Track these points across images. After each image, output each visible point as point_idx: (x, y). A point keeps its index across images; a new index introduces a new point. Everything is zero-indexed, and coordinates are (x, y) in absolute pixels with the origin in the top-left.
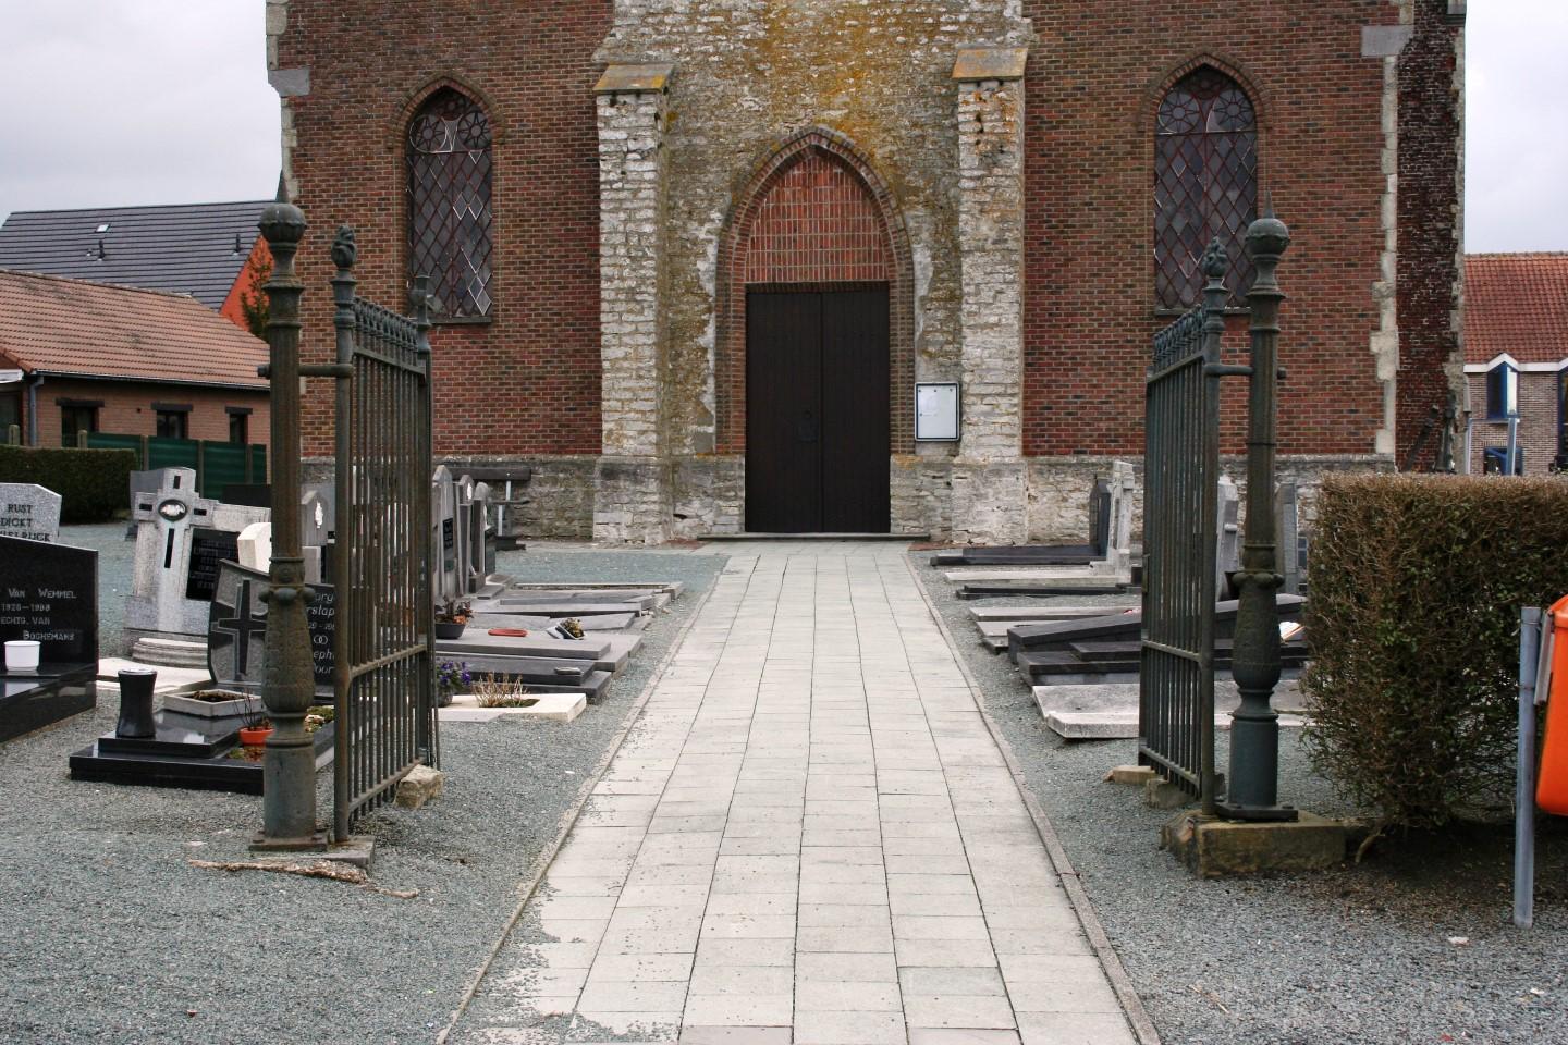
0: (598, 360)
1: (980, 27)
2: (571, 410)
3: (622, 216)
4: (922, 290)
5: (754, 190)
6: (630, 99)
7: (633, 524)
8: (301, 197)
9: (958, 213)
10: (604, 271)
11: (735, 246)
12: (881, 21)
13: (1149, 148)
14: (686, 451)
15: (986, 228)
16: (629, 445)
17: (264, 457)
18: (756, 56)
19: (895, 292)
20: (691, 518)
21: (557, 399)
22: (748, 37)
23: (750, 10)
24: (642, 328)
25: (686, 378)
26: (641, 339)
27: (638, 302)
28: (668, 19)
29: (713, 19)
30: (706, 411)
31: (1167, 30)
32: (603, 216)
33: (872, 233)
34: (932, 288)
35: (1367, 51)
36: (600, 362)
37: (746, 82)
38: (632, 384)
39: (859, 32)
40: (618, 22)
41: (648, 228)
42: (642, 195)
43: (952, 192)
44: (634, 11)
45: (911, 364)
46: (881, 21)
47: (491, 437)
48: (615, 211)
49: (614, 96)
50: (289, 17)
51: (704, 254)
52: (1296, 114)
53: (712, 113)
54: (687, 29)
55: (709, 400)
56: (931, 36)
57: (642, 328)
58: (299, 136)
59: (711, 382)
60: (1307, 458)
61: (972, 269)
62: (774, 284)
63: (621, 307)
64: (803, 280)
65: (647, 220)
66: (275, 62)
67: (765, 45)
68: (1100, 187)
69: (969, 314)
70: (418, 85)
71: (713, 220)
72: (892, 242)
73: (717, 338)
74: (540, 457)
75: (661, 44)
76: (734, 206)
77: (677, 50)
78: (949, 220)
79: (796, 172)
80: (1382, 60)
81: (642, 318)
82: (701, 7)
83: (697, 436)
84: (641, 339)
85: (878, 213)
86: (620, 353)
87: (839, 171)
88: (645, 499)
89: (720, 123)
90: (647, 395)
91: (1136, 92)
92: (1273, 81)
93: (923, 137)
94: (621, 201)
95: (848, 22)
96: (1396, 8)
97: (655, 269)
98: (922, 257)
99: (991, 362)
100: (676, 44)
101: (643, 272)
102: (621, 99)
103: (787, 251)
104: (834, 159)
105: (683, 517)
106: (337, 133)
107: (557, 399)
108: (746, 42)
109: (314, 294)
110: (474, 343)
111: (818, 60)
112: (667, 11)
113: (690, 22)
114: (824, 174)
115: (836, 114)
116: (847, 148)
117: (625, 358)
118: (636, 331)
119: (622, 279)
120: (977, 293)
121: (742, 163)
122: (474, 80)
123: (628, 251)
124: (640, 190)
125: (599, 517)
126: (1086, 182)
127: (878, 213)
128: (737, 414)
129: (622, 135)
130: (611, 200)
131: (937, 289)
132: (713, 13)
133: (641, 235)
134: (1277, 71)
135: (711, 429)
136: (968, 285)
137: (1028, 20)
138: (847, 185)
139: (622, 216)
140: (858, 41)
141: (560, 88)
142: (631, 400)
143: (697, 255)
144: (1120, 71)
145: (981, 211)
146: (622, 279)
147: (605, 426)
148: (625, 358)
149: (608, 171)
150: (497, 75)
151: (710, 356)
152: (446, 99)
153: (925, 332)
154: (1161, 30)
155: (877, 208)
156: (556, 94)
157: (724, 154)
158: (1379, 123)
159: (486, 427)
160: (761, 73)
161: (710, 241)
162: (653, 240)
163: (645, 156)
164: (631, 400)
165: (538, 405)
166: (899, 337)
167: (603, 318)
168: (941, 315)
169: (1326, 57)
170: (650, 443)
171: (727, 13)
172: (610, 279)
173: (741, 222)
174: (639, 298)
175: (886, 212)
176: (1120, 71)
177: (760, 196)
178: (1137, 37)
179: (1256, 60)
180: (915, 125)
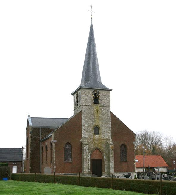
4: (105, 160)
13: (120, 149)
15: (112, 155)
17: (39, 173)
35: (133, 143)
61: (111, 158)
70: (66, 142)
122: (70, 142)
138: (99, 152)
149: (84, 150)
152: (68, 143)
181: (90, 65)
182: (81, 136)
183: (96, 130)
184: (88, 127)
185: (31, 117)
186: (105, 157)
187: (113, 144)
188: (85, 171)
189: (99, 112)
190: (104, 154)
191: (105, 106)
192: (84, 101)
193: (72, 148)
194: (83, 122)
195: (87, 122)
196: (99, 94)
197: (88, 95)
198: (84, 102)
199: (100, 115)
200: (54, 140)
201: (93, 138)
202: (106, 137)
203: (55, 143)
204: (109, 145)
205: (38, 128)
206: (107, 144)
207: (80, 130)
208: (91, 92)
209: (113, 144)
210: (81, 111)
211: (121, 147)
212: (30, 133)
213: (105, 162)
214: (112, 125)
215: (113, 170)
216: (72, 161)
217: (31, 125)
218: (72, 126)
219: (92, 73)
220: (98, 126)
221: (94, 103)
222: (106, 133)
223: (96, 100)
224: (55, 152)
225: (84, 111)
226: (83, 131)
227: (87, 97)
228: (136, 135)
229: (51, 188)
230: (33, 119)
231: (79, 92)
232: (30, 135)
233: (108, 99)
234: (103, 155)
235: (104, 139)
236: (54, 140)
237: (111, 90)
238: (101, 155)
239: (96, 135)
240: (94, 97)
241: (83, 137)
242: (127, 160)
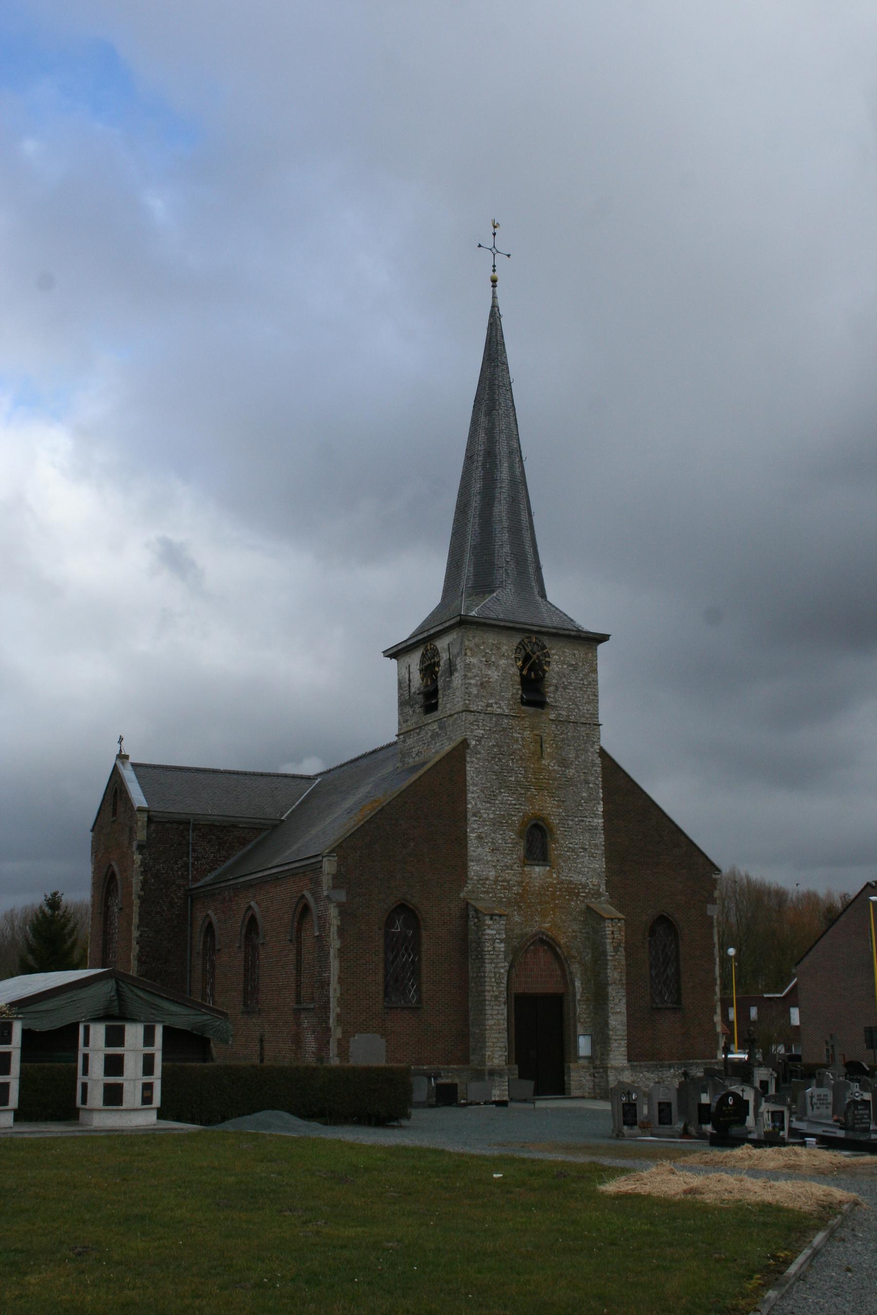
1: (593, 895)
4: (578, 997)
6: (497, 918)
13: (647, 945)
15: (616, 975)
16: (496, 1061)
24: (500, 1012)
26: (500, 1017)
28: (487, 882)
32: (487, 965)
34: (582, 996)
37: (515, 910)
38: (497, 1035)
39: (554, 893)
41: (502, 971)
48: (491, 963)
49: (492, 916)
57: (500, 1012)
58: (342, 920)
60: (699, 1061)
61: (611, 990)
63: (493, 1003)
67: (521, 895)
74: (441, 1066)
84: (500, 1017)
90: (502, 1040)
93: (576, 936)
94: (493, 959)
99: (619, 1027)
100: (490, 893)
102: (494, 917)
111: (540, 903)
112: (487, 879)
115: (547, 925)
116: (553, 940)
118: (498, 1014)
119: (493, 991)
129: (494, 932)
132: (503, 881)
133: (500, 973)
146: (493, 991)
149: (488, 947)
160: (520, 907)
163: (502, 941)
168: (584, 1007)
172: (489, 991)
180: (573, 931)
181: (496, 510)
182: (465, 868)
183: (537, 840)
184: (497, 824)
185: (135, 766)
186: (578, 984)
187: (621, 916)
188: (491, 1058)
190: (575, 968)
191: (572, 718)
192: (475, 691)
193: (424, 934)
194: (474, 798)
195: (490, 798)
196: (547, 655)
198: (476, 696)
199: (553, 765)
200: (334, 887)
201: (520, 883)
202: (584, 880)
203: (340, 905)
204: (603, 919)
205: (180, 823)
206: (592, 916)
207: (462, 841)
208: (508, 645)
209: (621, 916)
210: (466, 740)
211: (652, 932)
212: (141, 848)
213: (581, 1010)
214: (606, 815)
215: (624, 1049)
216: (419, 1001)
217: (145, 805)
218: (409, 812)
219: (507, 549)
220: (543, 819)
221: (524, 702)
222: (583, 860)
223: (533, 689)
224: (340, 951)
225: (479, 740)
226: (474, 849)
227: (485, 671)
228: (719, 870)
229: (788, 1177)
230: (138, 769)
231: (441, 644)
232: (137, 858)
233: (590, 683)
234: (571, 973)
235: (572, 891)
236: (334, 887)
237: (604, 638)
238: (559, 973)
239: (537, 869)
240: (525, 672)
241: (471, 874)
242: (678, 1001)
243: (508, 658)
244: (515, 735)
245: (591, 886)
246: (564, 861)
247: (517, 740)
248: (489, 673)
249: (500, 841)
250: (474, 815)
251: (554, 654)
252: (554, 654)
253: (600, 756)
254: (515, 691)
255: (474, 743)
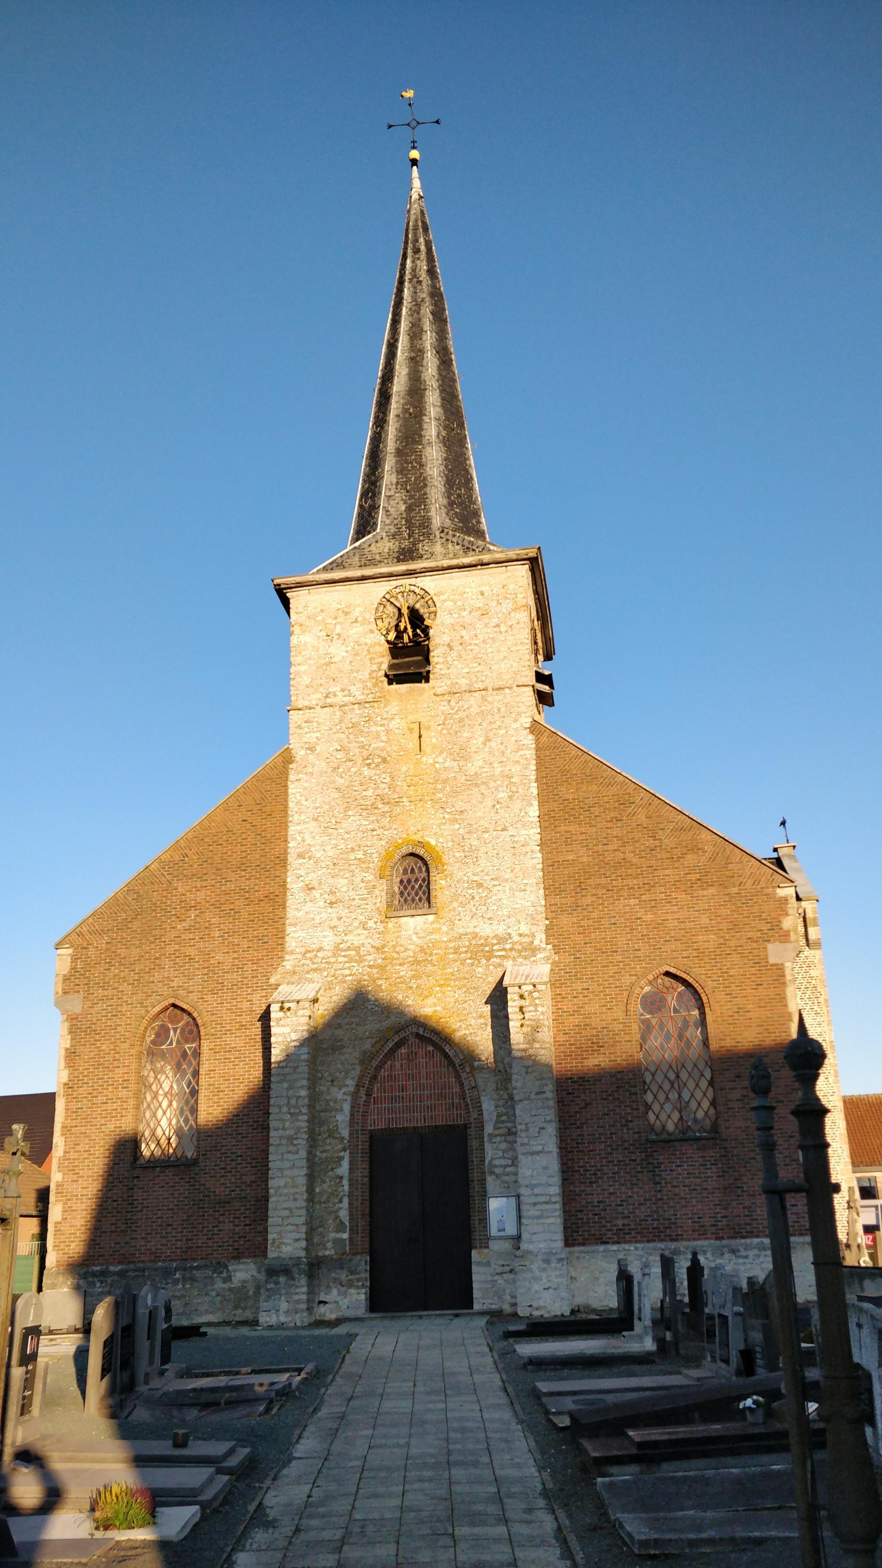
0: (267, 1189)
1: (519, 951)
2: (247, 1225)
3: (285, 1085)
4: (489, 1129)
5: (375, 1063)
7: (288, 1311)
8: (70, 1081)
9: (511, 1075)
10: (272, 1124)
11: (362, 1103)
12: (456, 951)
14: (327, 1253)
18: (376, 975)
19: (472, 1131)
20: (330, 1303)
21: (238, 1218)
22: (371, 963)
23: (373, 947)
25: (328, 1201)
26: (296, 1172)
27: (295, 1145)
28: (320, 954)
29: (347, 953)
30: (342, 1223)
31: (639, 950)
33: (454, 1090)
35: (772, 960)
36: (268, 1189)
40: (287, 957)
42: (298, 1070)
43: (507, 1060)
44: (298, 950)
45: (483, 1182)
46: (456, 951)
47: (190, 1247)
50: (72, 962)
51: (342, 1109)
52: (730, 1001)
53: (348, 1013)
54: (332, 960)
55: (344, 1214)
56: (488, 960)
59: (346, 1200)
62: (389, 1129)
63: (282, 1149)
64: (409, 1125)
65: (302, 1087)
66: (60, 991)
68: (605, 1054)
69: (522, 1145)
71: (348, 1086)
72: (468, 1095)
73: (350, 1169)
75: (315, 970)
76: (361, 1077)
77: (325, 974)
78: (505, 1080)
79: (403, 1051)
80: (782, 964)
81: (297, 1156)
82: (341, 946)
83: (336, 1241)
85: (458, 1077)
86: (282, 1182)
87: (431, 1048)
88: (297, 1290)
89: (353, 1020)
91: (624, 990)
92: (713, 981)
95: (435, 952)
96: (788, 931)
97: (308, 1121)
98: (488, 1106)
100: (324, 969)
101: (299, 1123)
103: (397, 1105)
104: (429, 1041)
105: (325, 1303)
106: (97, 1037)
107: (238, 1218)
108: (370, 967)
109: (73, 1148)
110: (182, 1179)
112: (320, 949)
113: (334, 955)
114: (421, 1052)
117: (286, 1186)
120: (527, 1130)
121: (367, 1045)
123: (289, 1109)
124: (298, 1067)
125: (264, 1305)
126: (595, 1051)
127: (458, 1077)
128: (363, 1223)
130: (278, 1075)
131: (500, 1128)
132: (349, 949)
134: (715, 973)
135: (345, 1236)
136: (520, 1124)
137: (550, 947)
139: (285, 1085)
140: (442, 963)
141: (248, 1001)
142: (288, 1217)
143: (337, 1110)
144: (611, 977)
145: (527, 1073)
147: (270, 1237)
148: (286, 1186)
150: (206, 994)
151: (345, 1182)
153: (492, 1159)
154: (636, 950)
155: (457, 1072)
156: (245, 1005)
157: (355, 1040)
158: (786, 1005)
159: (187, 1240)
161: (346, 1100)
162: (306, 1101)
164: (288, 1217)
165: (224, 1222)
166: (475, 1163)
167: (271, 1158)
168: (503, 1146)
169: (745, 964)
170: (301, 1248)
171: (357, 949)
173: (366, 1086)
174: (295, 1142)
175: (464, 1076)
176: (611, 977)
177: (379, 1068)
178: (621, 955)
179: (700, 967)
182: (280, 937)
189: (431, 738)
197: (338, 629)
199: (444, 761)
241: (291, 943)
243: (365, 621)
244: (373, 729)
245: (516, 938)
246: (462, 905)
247: (377, 736)
248: (332, 650)
249: (344, 889)
250: (300, 856)
251: (445, 601)
252: (445, 601)
253: (532, 732)
254: (375, 667)
255: (303, 752)
